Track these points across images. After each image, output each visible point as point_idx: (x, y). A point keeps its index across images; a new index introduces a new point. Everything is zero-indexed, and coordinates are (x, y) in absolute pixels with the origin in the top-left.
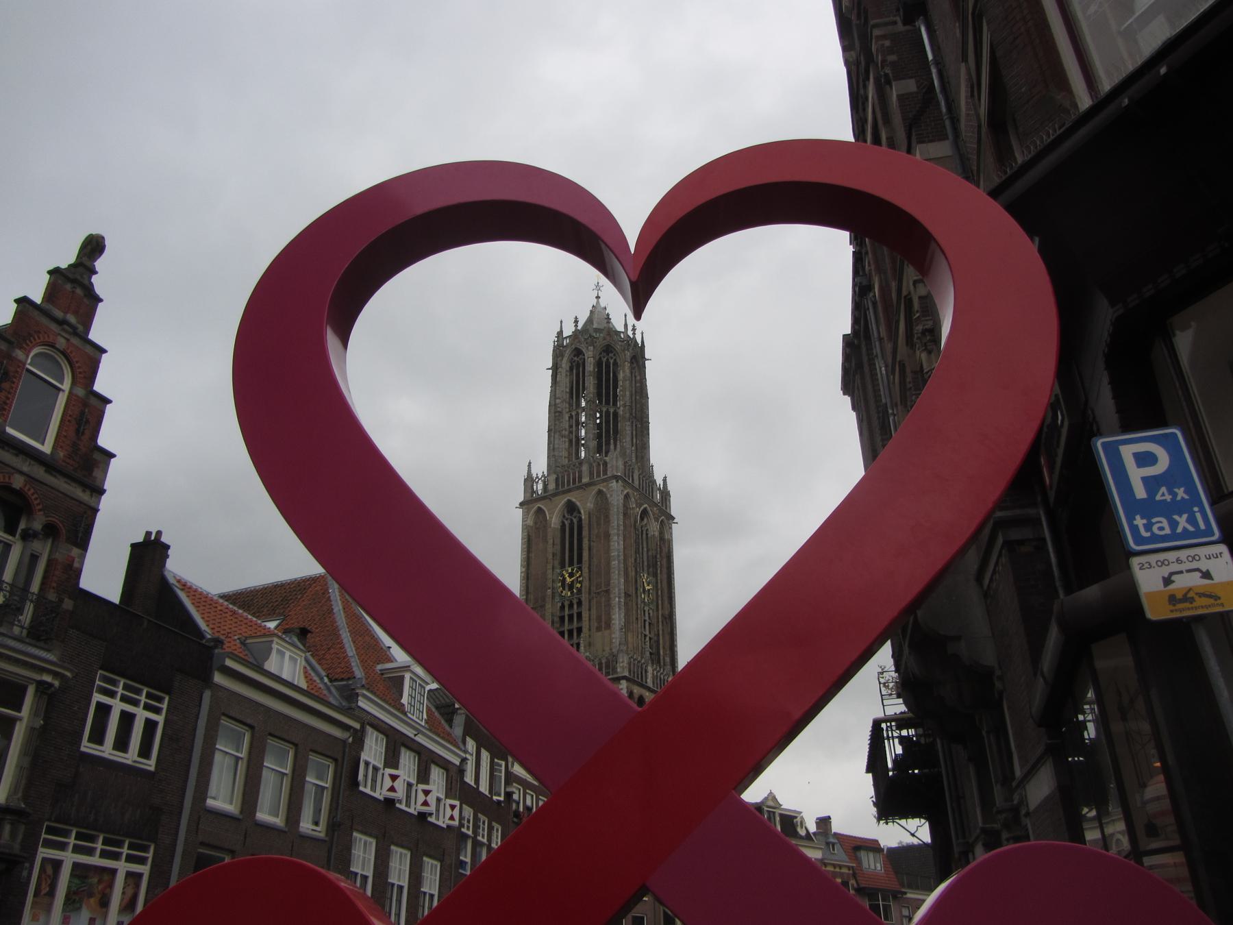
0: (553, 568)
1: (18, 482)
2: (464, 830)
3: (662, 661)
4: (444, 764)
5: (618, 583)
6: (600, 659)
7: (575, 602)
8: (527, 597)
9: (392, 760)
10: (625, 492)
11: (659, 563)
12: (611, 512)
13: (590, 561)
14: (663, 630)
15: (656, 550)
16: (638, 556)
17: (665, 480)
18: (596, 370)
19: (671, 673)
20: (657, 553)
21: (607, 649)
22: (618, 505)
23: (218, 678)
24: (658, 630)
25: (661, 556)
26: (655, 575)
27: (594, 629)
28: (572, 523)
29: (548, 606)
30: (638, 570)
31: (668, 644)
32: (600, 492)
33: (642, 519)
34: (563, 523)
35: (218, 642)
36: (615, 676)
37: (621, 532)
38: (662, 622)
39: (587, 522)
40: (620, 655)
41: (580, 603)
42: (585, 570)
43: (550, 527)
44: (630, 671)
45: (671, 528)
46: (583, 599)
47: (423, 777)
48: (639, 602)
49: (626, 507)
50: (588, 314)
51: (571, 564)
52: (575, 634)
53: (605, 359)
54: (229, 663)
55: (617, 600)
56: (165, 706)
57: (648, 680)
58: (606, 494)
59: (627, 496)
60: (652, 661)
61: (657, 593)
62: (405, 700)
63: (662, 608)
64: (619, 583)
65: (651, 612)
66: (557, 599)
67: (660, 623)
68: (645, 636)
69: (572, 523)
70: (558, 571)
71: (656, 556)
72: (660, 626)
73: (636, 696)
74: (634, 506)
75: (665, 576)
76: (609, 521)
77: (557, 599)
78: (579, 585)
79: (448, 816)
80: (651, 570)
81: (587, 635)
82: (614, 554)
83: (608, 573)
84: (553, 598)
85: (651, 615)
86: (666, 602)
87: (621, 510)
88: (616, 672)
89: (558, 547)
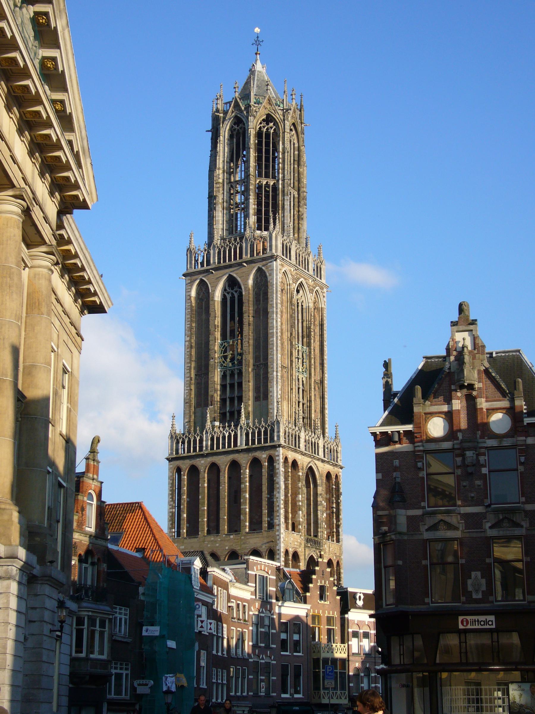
2: (214, 633)
7: (236, 372)
10: (283, 271)
11: (312, 333)
16: (294, 330)
18: (257, 141)
19: (322, 436)
20: (311, 323)
24: (310, 397)
30: (294, 343)
31: (318, 410)
33: (298, 291)
38: (315, 389)
52: (236, 402)
53: (265, 130)
57: (301, 445)
58: (265, 272)
61: (310, 362)
63: (315, 375)
65: (304, 379)
67: (313, 389)
68: (299, 402)
72: (313, 392)
73: (290, 461)
74: (291, 282)
75: (318, 343)
78: (240, 357)
79: (209, 628)
80: (305, 340)
85: (305, 382)
88: (272, 439)
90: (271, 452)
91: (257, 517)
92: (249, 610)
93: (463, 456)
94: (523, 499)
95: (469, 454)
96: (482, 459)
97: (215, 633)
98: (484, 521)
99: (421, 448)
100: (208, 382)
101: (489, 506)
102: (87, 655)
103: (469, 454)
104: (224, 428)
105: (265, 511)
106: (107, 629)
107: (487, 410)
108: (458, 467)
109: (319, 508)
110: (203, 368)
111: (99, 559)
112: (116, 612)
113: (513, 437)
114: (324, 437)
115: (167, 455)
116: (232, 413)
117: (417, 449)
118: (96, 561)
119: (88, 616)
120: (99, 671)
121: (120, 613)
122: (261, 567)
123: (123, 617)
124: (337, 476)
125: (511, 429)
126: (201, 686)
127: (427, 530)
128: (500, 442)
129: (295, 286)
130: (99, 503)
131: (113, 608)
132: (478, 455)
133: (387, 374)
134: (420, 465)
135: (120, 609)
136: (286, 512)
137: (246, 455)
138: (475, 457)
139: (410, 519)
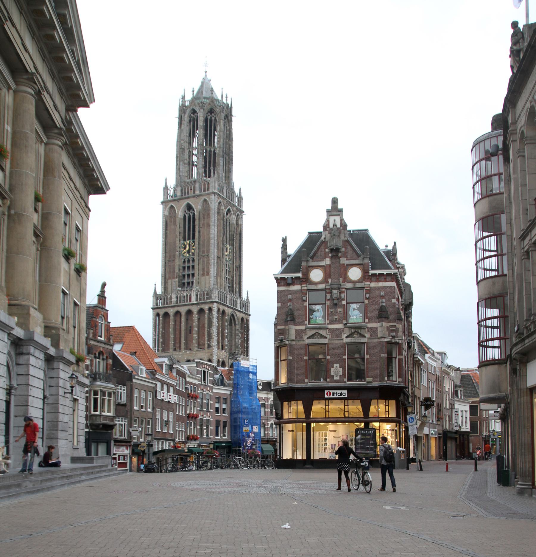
0: (180, 240)
1: (101, 349)
3: (234, 291)
4: (172, 386)
5: (214, 252)
6: (204, 292)
7: (191, 259)
8: (165, 254)
9: (162, 389)
10: (219, 201)
11: (235, 239)
12: (211, 213)
13: (199, 238)
14: (236, 274)
15: (234, 231)
17: (240, 190)
21: (207, 286)
22: (215, 208)
23: (134, 380)
24: (233, 275)
25: (236, 234)
26: (233, 245)
27: (200, 275)
28: (190, 216)
29: (177, 261)
32: (205, 200)
33: (227, 214)
34: (185, 215)
35: (132, 372)
36: (211, 300)
37: (216, 224)
39: (198, 216)
40: (214, 290)
41: (193, 260)
42: (197, 243)
43: (178, 217)
44: (219, 297)
45: (242, 218)
46: (195, 258)
47: (168, 391)
48: (224, 260)
49: (219, 209)
50: (200, 84)
51: (189, 239)
54: (136, 377)
55: (213, 261)
56: (125, 389)
57: (227, 302)
59: (220, 203)
60: (230, 292)
61: (233, 255)
62: (164, 372)
64: (214, 252)
65: (230, 265)
66: (182, 257)
67: (234, 271)
69: (190, 216)
70: (182, 242)
71: (234, 235)
73: (221, 310)
74: (223, 208)
75: (238, 245)
76: (210, 217)
77: (182, 257)
78: (193, 251)
81: (197, 278)
82: (212, 236)
83: (209, 246)
84: (179, 256)
86: (238, 259)
87: (216, 212)
88: (211, 298)
89: (182, 229)
90: (211, 305)
91: (202, 342)
92: (198, 390)
93: (331, 293)
94: (367, 320)
95: (335, 292)
96: (343, 295)
97: (178, 402)
98: (342, 333)
99: (306, 288)
100: (175, 265)
101: (346, 324)
102: (100, 413)
103: (335, 292)
104: (184, 291)
105: (207, 338)
106: (112, 398)
107: (347, 265)
108: (328, 300)
109: (237, 337)
110: (172, 257)
111: (107, 357)
112: (118, 389)
113: (362, 282)
114: (240, 298)
115: (152, 306)
116: (188, 283)
117: (303, 288)
118: (105, 357)
119: (101, 390)
120: (108, 422)
121: (121, 389)
122: (204, 366)
123: (122, 391)
124: (247, 320)
125: (361, 277)
126: (170, 432)
127: (308, 338)
128: (354, 285)
129: (226, 211)
130: (106, 323)
131: (116, 386)
132: (340, 293)
133: (284, 247)
134: (304, 298)
135: (121, 387)
136: (218, 339)
137: (197, 307)
138: (338, 294)
139: (297, 331)
